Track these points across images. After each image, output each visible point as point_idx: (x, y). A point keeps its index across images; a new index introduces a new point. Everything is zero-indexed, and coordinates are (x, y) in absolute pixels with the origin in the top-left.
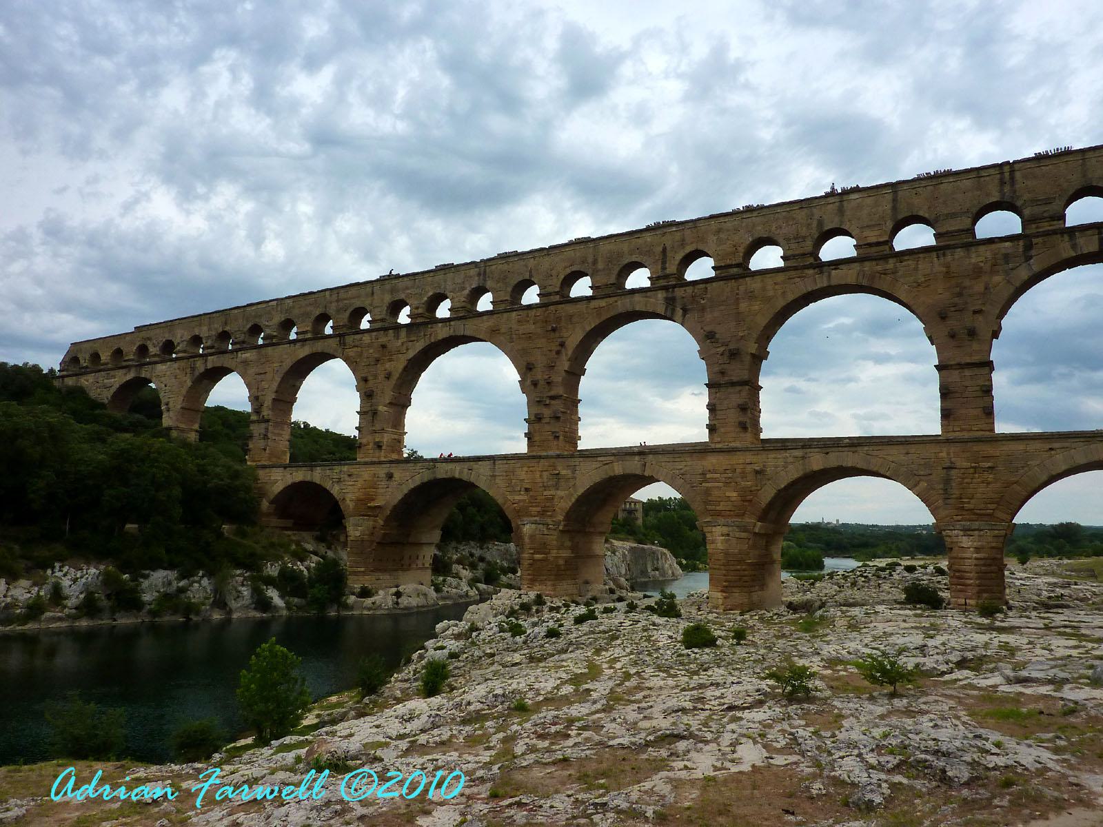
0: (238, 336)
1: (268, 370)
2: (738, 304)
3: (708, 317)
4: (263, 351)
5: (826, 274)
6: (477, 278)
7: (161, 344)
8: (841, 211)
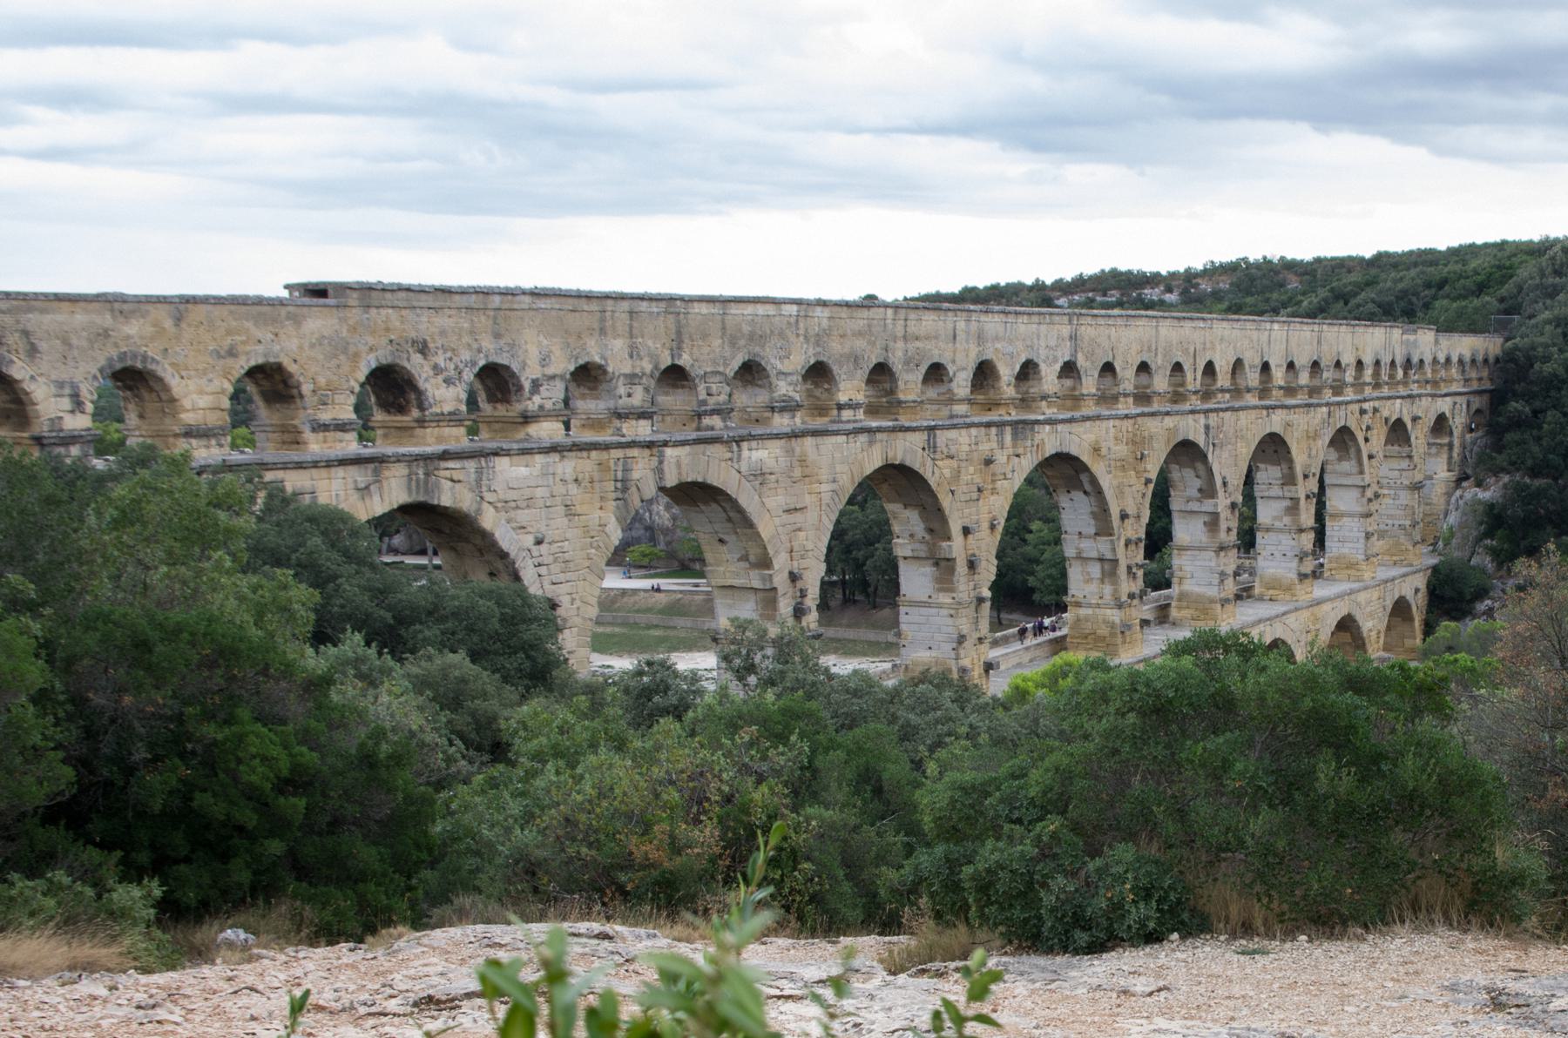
1: (808, 500)
7: (469, 375)
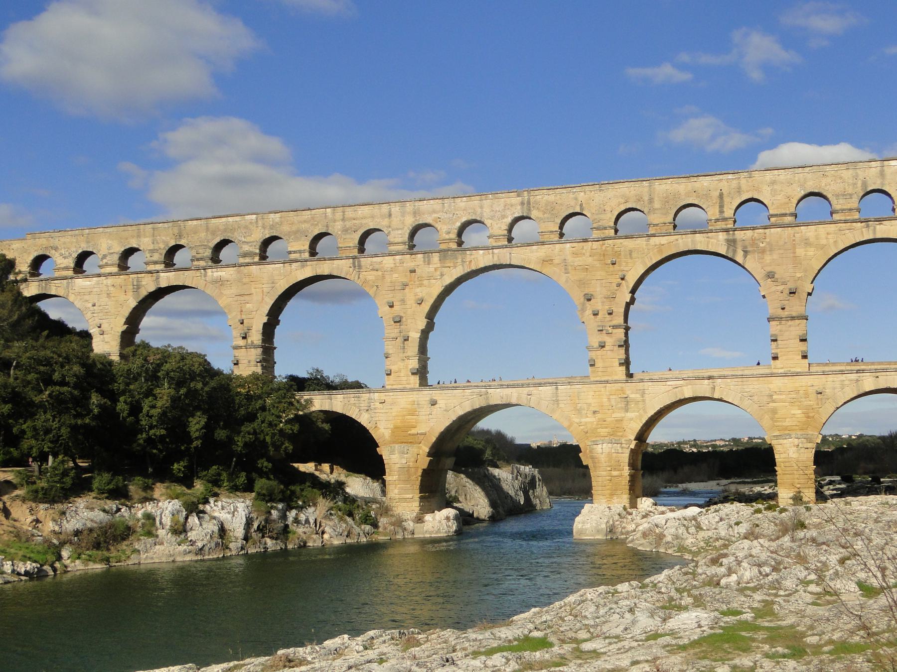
0: (200, 251)
1: (253, 291)
2: (794, 248)
3: (768, 258)
4: (245, 270)
5: (872, 228)
6: (519, 207)
7: (75, 255)
8: (882, 174)
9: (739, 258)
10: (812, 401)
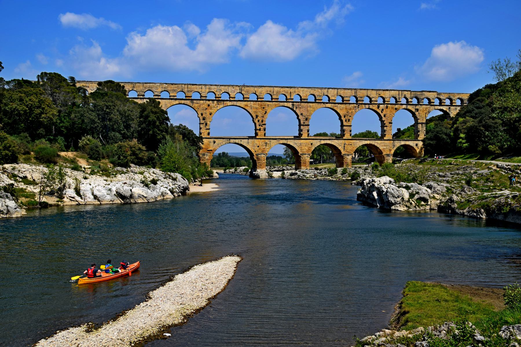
8: (328, 92)
9: (295, 109)
10: (310, 146)
